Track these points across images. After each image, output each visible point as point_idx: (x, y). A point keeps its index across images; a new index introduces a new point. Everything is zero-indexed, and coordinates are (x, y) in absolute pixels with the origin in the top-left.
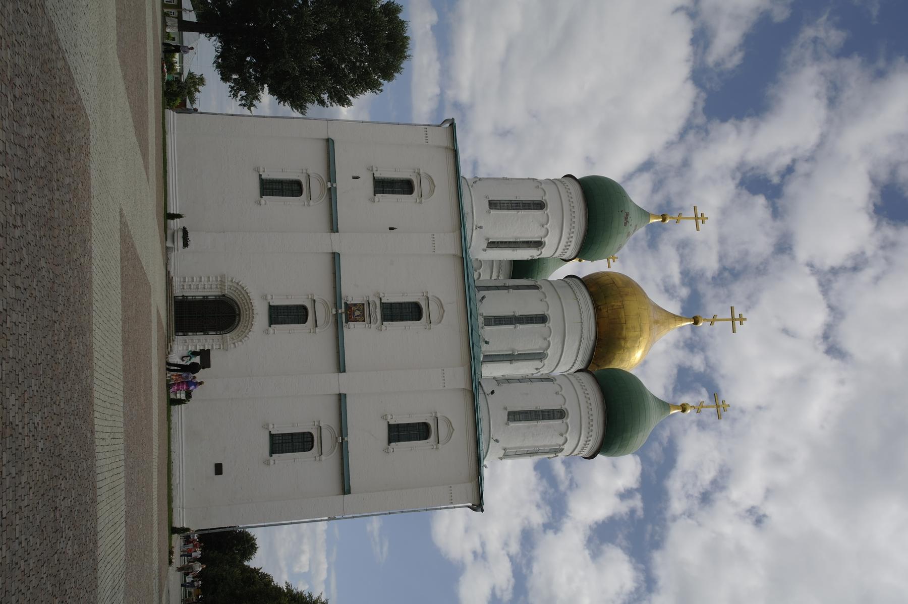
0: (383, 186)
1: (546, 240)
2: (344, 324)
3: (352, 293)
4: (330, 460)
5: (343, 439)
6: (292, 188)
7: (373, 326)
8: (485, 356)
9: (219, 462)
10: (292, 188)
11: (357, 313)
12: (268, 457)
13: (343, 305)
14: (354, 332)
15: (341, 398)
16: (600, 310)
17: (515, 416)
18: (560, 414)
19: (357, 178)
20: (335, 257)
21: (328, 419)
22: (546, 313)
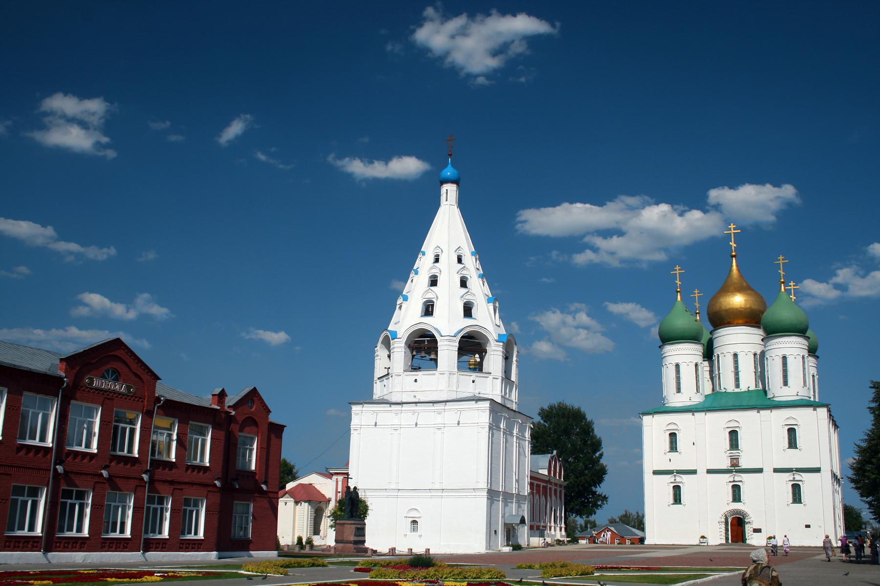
0: (673, 447)
1: (694, 362)
2: (740, 468)
3: (726, 464)
4: (805, 476)
5: (794, 471)
6: (677, 489)
7: (741, 454)
8: (756, 387)
9: (805, 526)
10: (677, 489)
11: (735, 461)
12: (803, 504)
13: (731, 468)
14: (744, 464)
15: (776, 470)
16: (729, 322)
17: (785, 383)
18: (784, 358)
19: (670, 460)
20: (709, 472)
21: (788, 476)
22: (733, 354)
